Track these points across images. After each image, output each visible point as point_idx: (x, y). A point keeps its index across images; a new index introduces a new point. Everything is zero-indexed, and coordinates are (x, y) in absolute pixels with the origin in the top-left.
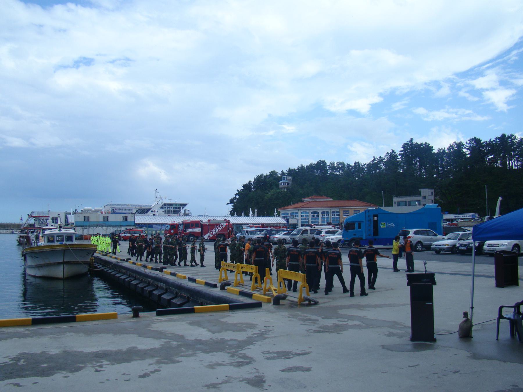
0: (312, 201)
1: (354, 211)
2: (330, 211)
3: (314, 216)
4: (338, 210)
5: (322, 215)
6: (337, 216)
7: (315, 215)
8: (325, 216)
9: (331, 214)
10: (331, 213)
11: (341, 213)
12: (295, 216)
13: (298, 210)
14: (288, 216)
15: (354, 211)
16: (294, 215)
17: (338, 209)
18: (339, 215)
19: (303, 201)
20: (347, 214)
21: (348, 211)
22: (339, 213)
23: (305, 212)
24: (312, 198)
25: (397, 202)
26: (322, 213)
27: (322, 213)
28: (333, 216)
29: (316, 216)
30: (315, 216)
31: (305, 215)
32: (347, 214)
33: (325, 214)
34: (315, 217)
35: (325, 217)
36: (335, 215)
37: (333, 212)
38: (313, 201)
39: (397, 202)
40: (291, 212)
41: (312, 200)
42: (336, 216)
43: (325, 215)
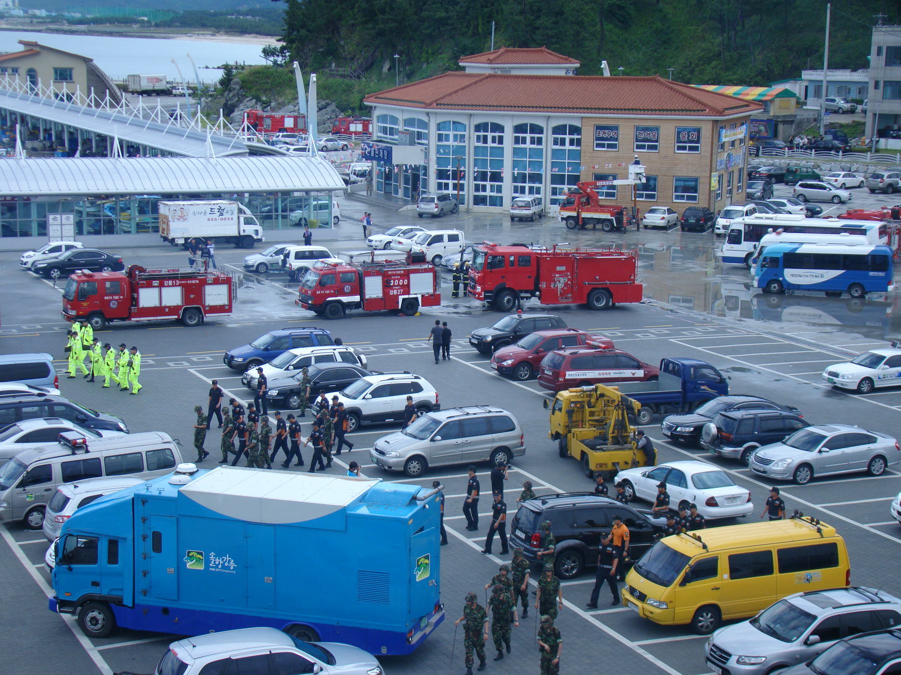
0: (491, 72)
1: (637, 128)
2: (548, 122)
3: (485, 141)
4: (577, 123)
5: (517, 140)
6: (572, 142)
7: (490, 135)
8: (525, 143)
9: (548, 137)
10: (550, 131)
11: (588, 135)
12: (420, 135)
13: (428, 114)
14: (398, 132)
15: (637, 128)
16: (416, 130)
17: (578, 117)
18: (579, 142)
19: (464, 68)
20: (611, 139)
21: (616, 128)
22: (579, 133)
23: (454, 122)
24: (490, 61)
25: (888, 48)
26: (519, 129)
27: (519, 129)
28: (555, 143)
29: (494, 141)
30: (489, 139)
31: (451, 134)
32: (611, 139)
33: (528, 136)
34: (490, 144)
35: (528, 145)
36: (563, 142)
37: (558, 130)
38: (499, 73)
39: (888, 48)
40: (407, 116)
41: (494, 68)
42: (567, 147)
43: (528, 141)
